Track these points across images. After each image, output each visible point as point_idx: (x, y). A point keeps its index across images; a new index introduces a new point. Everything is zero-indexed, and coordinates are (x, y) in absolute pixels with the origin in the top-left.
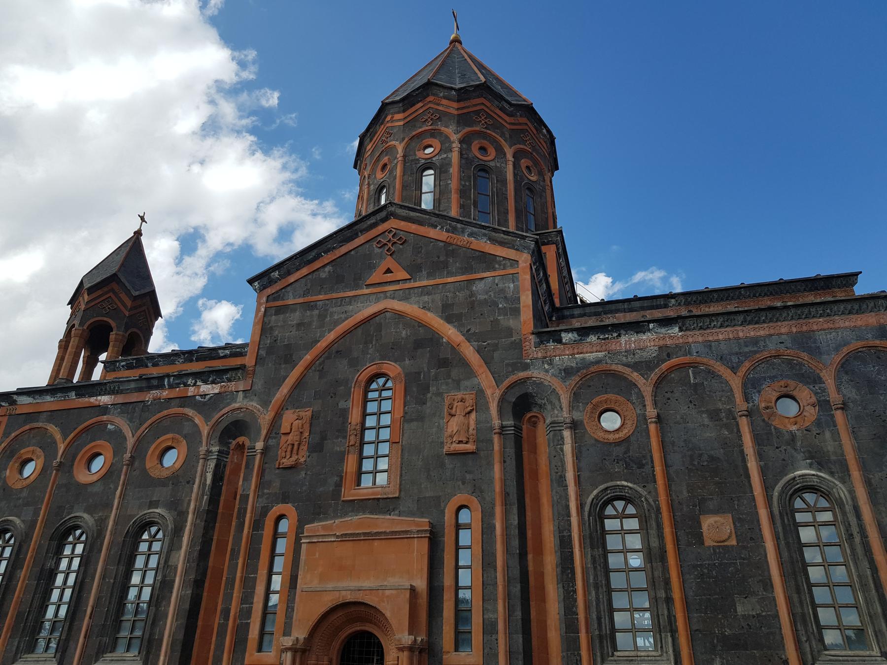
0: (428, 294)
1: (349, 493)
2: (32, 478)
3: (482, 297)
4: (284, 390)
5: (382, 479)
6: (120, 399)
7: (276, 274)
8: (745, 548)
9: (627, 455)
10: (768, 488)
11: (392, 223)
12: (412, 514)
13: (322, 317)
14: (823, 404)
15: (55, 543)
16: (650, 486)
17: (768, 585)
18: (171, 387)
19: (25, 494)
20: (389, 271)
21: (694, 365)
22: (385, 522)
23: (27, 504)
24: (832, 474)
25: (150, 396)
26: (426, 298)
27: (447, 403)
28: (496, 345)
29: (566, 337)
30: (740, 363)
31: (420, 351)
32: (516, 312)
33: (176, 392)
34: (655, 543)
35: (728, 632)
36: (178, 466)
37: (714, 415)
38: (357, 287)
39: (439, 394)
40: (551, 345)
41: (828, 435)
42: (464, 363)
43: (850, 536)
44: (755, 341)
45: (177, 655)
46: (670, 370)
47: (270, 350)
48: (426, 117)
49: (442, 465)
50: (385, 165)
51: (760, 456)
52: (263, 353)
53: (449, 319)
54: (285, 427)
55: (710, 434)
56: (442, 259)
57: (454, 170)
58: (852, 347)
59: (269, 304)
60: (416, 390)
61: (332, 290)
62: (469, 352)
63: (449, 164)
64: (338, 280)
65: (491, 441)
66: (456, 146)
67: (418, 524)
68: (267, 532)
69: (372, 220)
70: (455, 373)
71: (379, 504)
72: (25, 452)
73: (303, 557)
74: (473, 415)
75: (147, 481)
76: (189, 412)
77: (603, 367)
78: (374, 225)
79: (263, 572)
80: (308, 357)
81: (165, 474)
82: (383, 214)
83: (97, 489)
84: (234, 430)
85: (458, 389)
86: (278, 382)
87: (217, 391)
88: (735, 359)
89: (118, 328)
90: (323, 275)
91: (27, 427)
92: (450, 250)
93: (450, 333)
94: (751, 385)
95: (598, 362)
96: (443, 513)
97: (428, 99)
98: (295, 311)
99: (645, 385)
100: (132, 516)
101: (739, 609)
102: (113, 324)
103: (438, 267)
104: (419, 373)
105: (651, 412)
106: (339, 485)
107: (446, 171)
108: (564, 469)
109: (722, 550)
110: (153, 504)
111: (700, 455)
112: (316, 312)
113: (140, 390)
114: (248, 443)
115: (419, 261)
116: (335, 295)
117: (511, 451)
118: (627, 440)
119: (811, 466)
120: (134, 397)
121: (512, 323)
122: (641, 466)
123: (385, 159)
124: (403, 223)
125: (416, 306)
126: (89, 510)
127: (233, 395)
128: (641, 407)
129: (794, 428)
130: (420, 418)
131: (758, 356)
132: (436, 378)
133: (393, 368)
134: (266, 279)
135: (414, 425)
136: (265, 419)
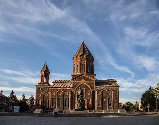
4: (76, 89)
6: (61, 89)
11: (84, 75)
13: (78, 83)
32: (93, 85)
33: (66, 89)
47: (74, 86)
51: (108, 96)
53: (88, 85)
57: (86, 65)
62: (90, 87)
64: (79, 80)
66: (86, 62)
76: (68, 90)
80: (77, 87)
84: (71, 92)
93: (88, 86)
94: (108, 92)
102: (47, 75)
105: (102, 93)
120: (62, 89)
127: (71, 89)
130: (86, 92)
136: (74, 92)
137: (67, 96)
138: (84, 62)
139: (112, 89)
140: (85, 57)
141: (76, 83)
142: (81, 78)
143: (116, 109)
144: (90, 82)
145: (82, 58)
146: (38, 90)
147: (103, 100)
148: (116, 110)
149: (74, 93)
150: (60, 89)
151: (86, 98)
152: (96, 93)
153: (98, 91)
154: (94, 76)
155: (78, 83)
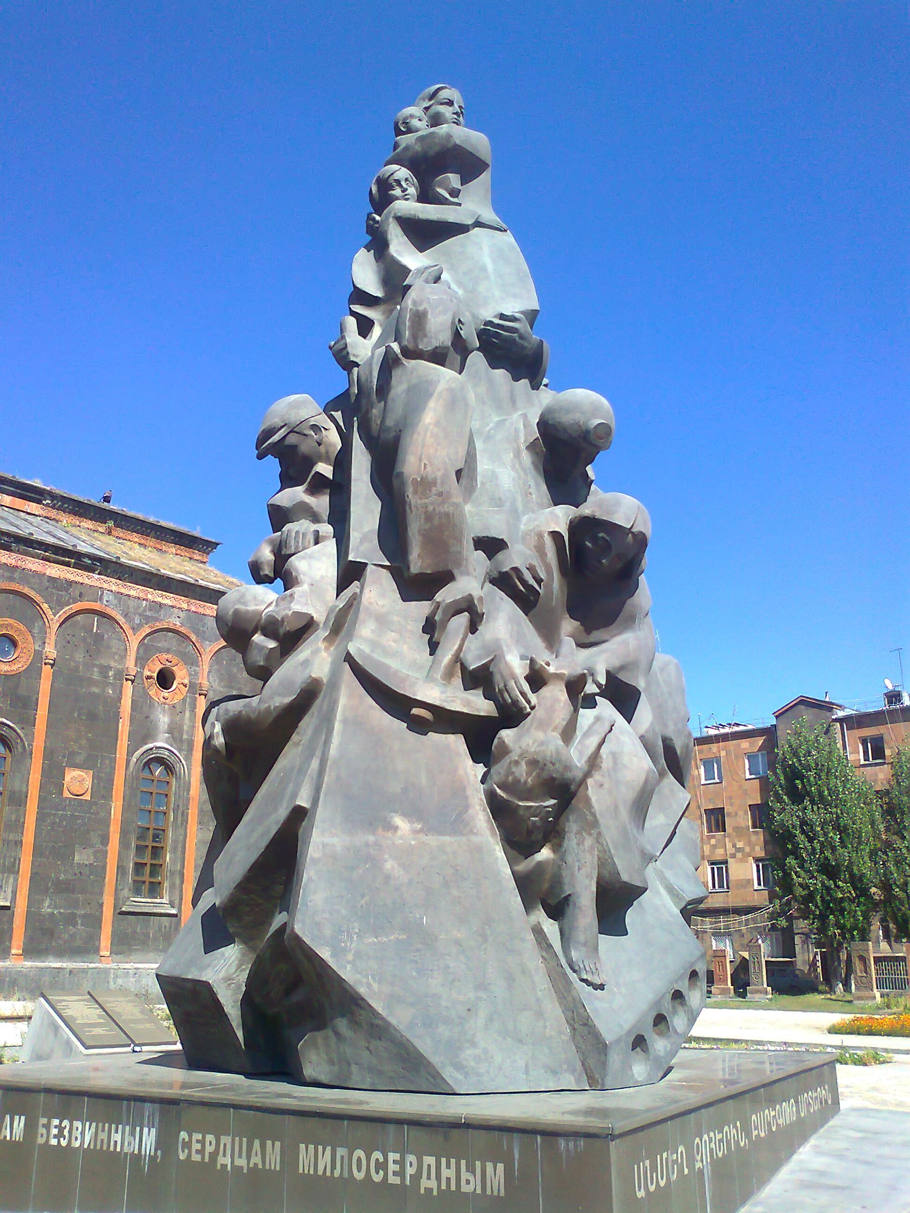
8: (95, 803)
10: (130, 753)
14: (194, 688)
17: (105, 840)
21: (103, 615)
24: (180, 751)
30: (141, 625)
35: (62, 877)
41: (187, 714)
46: (78, 613)
55: (95, 690)
88: (137, 621)
101: (77, 858)
105: (50, 651)
109: (77, 802)
118: (18, 675)
122: (25, 706)
128: (40, 643)
131: (158, 624)
147: (53, 776)
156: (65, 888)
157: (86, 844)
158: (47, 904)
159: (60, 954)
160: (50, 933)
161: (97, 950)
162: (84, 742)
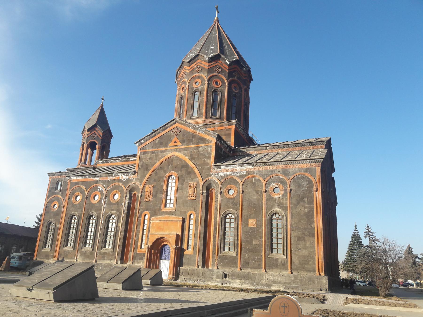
0: (186, 150)
1: (164, 209)
2: (80, 201)
3: (201, 152)
4: (146, 179)
5: (172, 206)
7: (143, 141)
9: (233, 203)
11: (177, 125)
12: (178, 215)
13: (156, 156)
14: (285, 190)
15: (88, 220)
16: (238, 211)
17: (261, 237)
18: (115, 176)
19: (78, 206)
20: (175, 142)
22: (171, 217)
23: (79, 209)
24: (283, 210)
25: (109, 178)
26: (186, 152)
27: (189, 185)
28: (204, 168)
29: (222, 167)
31: (183, 169)
32: (210, 158)
34: (236, 226)
35: (250, 248)
36: (118, 199)
37: (257, 192)
38: (166, 147)
39: (187, 182)
40: (218, 169)
41: (285, 199)
42: (195, 173)
43: (283, 226)
44: (272, 171)
45: (121, 249)
47: (142, 166)
48: (197, 70)
49: (187, 203)
50: (183, 88)
52: (140, 167)
53: (192, 159)
54: (146, 190)
55: (255, 197)
56: (191, 138)
58: (297, 174)
59: (142, 151)
60: (181, 181)
61: (159, 147)
62: (196, 170)
63: (204, 90)
64: (161, 144)
65: (200, 197)
67: (179, 218)
68: (142, 219)
69: (171, 123)
70: (192, 176)
71: (171, 213)
72: (77, 194)
73: (151, 226)
74: (196, 189)
75: (110, 203)
76: (120, 184)
77: (230, 177)
78: (172, 125)
79: (141, 229)
80: (152, 169)
81: (115, 202)
82: (174, 122)
83: (97, 205)
85: (192, 181)
86: (144, 176)
87: (128, 178)
88: (266, 176)
89: (99, 143)
90: (157, 142)
91: (76, 186)
92: (194, 136)
93: (191, 164)
95: (230, 175)
96: (186, 215)
97: (199, 61)
98: (148, 153)
99: (241, 183)
100: (107, 213)
102: (97, 142)
103: (190, 142)
104: (182, 176)
105: (241, 191)
106: (160, 207)
107: (203, 93)
108: (217, 205)
109: (253, 228)
110: (112, 210)
111: (252, 203)
112: (155, 154)
113: (106, 176)
114: (137, 193)
115: (184, 139)
116: (160, 149)
117: (204, 200)
118: (234, 198)
119: (278, 207)
120: (105, 179)
121: (209, 161)
122: (236, 205)
123: (183, 86)
124: (180, 125)
125: (182, 154)
126: (96, 211)
129: (276, 197)
130: (182, 189)
132: (187, 178)
133: (175, 174)
134: (140, 142)
135: (180, 191)
136: (141, 187)
137: (115, 204)
138: (199, 80)
139: (285, 172)
140: (204, 63)
141: (149, 156)
142: (170, 136)
143: (308, 271)
144: (198, 147)
145: (193, 70)
146: (52, 190)
148: (305, 274)
149: (140, 195)
150: (97, 179)
151: (178, 213)
152: (216, 191)
153: (228, 181)
154: (230, 127)
155: (156, 156)
156: (251, 251)
157: (256, 239)
158: (246, 255)
159: (251, 268)
160: (248, 263)
161: (262, 268)
162: (253, 212)
